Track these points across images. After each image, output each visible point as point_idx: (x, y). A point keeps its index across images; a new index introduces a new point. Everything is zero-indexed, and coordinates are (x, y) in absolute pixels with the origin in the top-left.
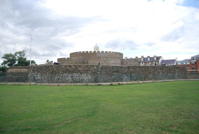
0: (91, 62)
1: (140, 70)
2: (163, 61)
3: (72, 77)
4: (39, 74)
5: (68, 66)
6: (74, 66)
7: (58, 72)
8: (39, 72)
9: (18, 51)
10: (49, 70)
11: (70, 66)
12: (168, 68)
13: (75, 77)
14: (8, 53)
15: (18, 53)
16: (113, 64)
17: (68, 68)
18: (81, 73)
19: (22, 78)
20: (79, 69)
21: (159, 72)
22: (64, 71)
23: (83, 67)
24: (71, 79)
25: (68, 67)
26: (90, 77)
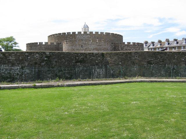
16: (94, 49)
18: (13, 65)
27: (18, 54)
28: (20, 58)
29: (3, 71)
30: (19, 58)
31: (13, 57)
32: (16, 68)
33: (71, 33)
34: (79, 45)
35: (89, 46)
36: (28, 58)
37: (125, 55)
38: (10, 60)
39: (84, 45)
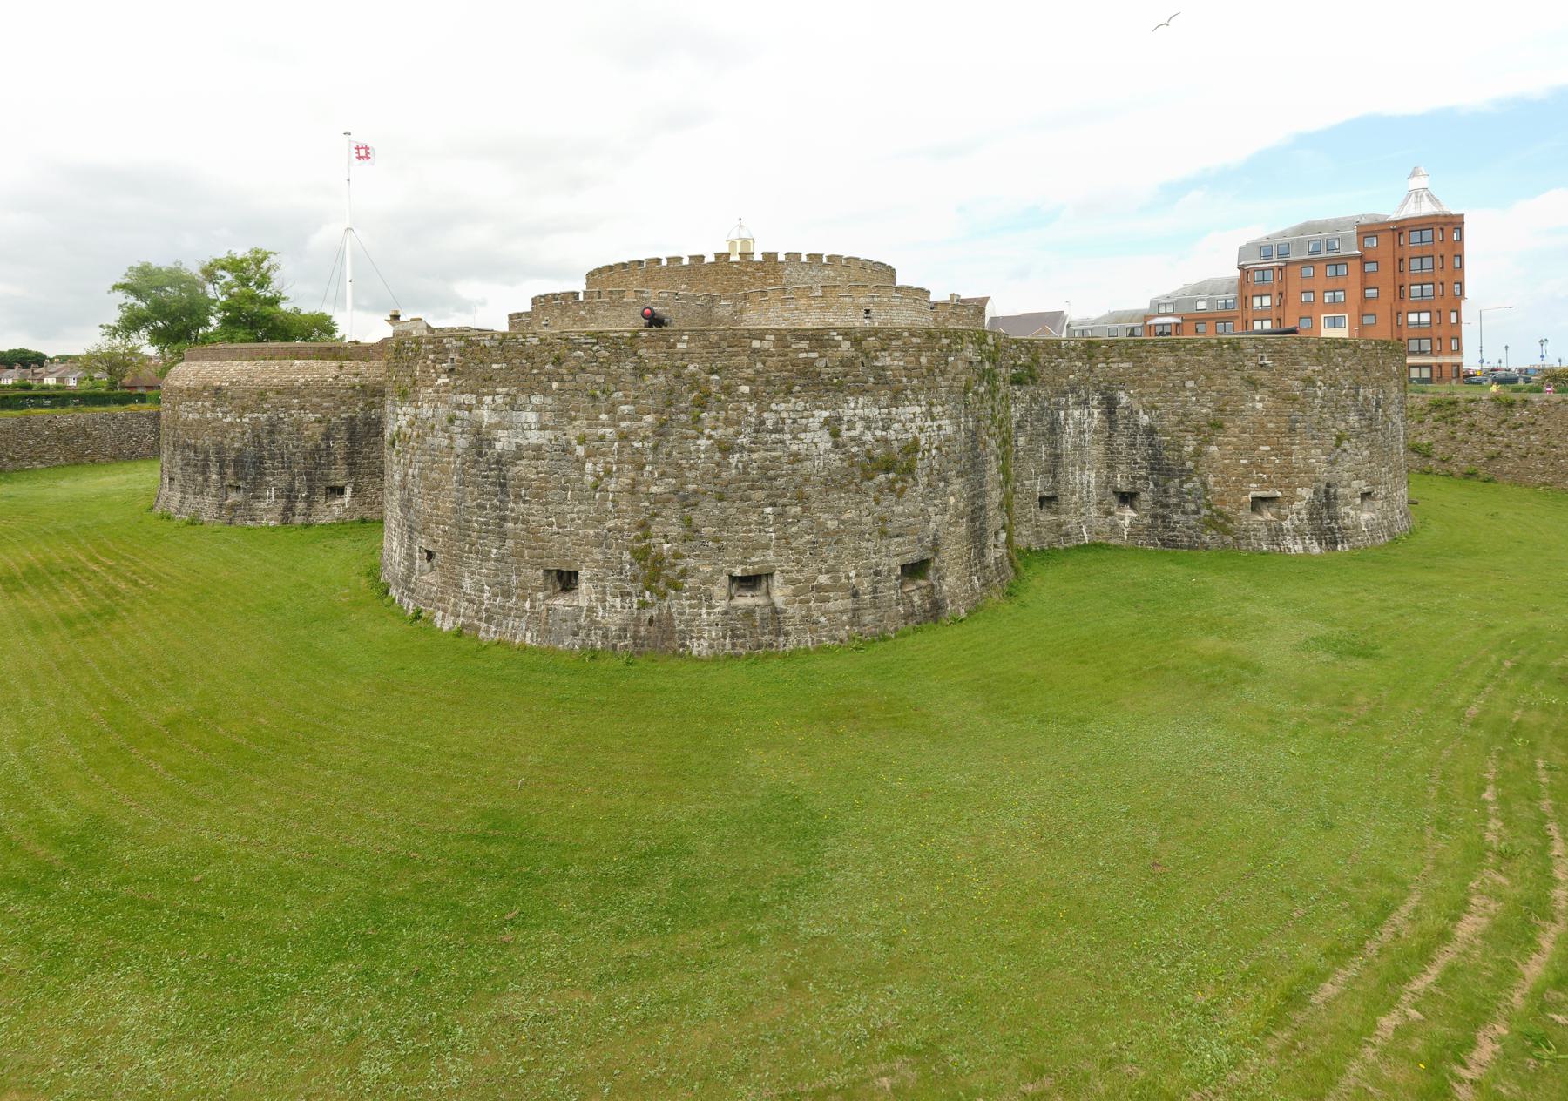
0: (769, 316)
1: (1180, 364)
2: (993, 319)
3: (833, 426)
4: (539, 410)
5: (802, 335)
6: (846, 333)
7: (727, 390)
8: (529, 391)
9: (222, 255)
10: (640, 371)
11: (818, 339)
12: (1355, 352)
13: (860, 426)
14: (161, 258)
15: (224, 268)
17: (803, 352)
18: (897, 397)
19: (299, 427)
20: (885, 360)
21: (1309, 381)
22: (768, 383)
23: (904, 349)
24: (824, 441)
25: (804, 344)
26: (949, 429)
27: (914, 340)
28: (923, 360)
29: (853, 433)
30: (918, 360)
31: (896, 354)
32: (907, 411)
33: (686, 262)
34: (857, 307)
35: (893, 313)
36: (947, 363)
37: (1211, 352)
38: (883, 369)
39: (874, 311)
